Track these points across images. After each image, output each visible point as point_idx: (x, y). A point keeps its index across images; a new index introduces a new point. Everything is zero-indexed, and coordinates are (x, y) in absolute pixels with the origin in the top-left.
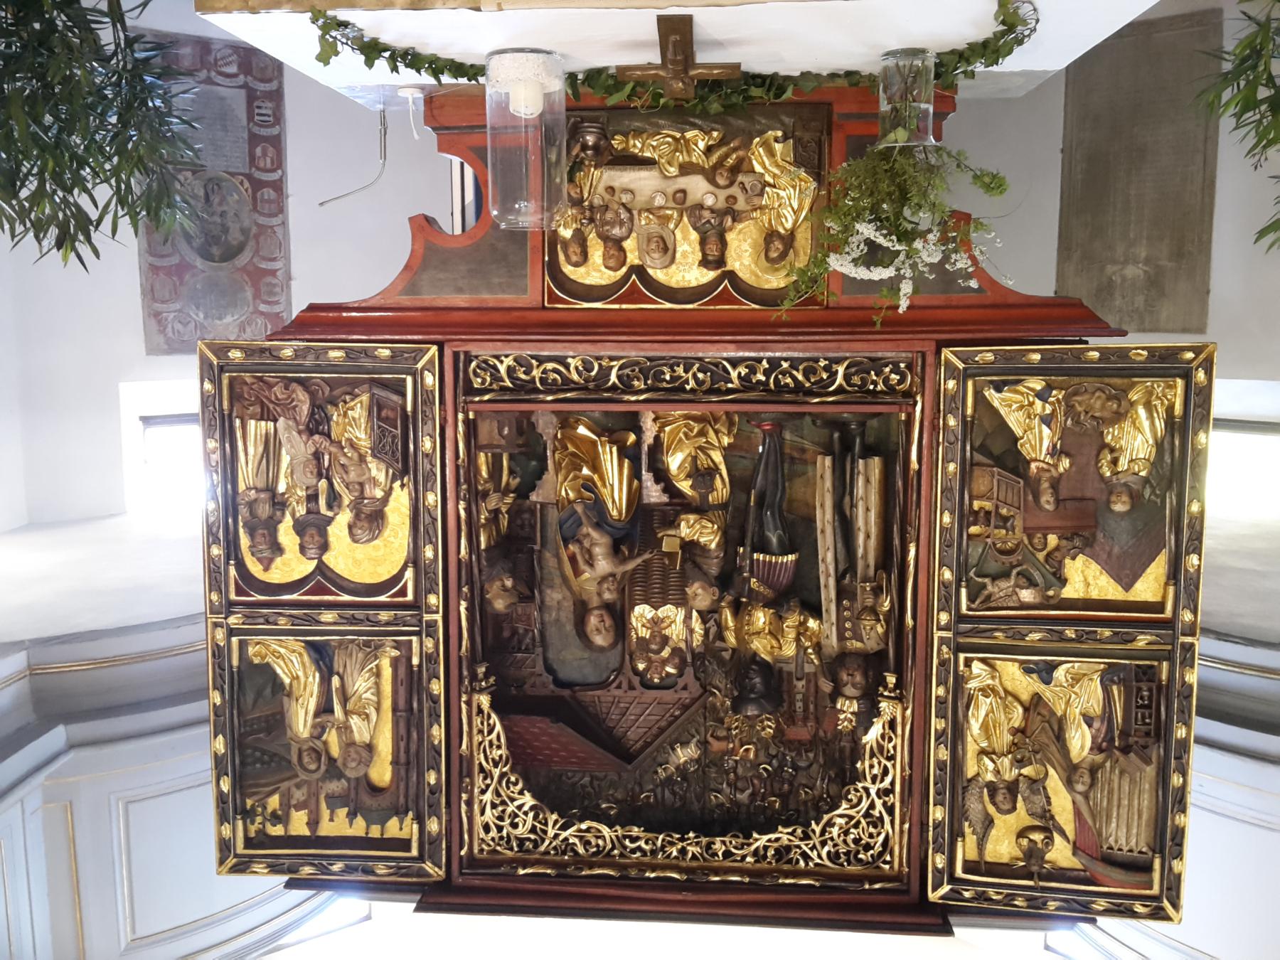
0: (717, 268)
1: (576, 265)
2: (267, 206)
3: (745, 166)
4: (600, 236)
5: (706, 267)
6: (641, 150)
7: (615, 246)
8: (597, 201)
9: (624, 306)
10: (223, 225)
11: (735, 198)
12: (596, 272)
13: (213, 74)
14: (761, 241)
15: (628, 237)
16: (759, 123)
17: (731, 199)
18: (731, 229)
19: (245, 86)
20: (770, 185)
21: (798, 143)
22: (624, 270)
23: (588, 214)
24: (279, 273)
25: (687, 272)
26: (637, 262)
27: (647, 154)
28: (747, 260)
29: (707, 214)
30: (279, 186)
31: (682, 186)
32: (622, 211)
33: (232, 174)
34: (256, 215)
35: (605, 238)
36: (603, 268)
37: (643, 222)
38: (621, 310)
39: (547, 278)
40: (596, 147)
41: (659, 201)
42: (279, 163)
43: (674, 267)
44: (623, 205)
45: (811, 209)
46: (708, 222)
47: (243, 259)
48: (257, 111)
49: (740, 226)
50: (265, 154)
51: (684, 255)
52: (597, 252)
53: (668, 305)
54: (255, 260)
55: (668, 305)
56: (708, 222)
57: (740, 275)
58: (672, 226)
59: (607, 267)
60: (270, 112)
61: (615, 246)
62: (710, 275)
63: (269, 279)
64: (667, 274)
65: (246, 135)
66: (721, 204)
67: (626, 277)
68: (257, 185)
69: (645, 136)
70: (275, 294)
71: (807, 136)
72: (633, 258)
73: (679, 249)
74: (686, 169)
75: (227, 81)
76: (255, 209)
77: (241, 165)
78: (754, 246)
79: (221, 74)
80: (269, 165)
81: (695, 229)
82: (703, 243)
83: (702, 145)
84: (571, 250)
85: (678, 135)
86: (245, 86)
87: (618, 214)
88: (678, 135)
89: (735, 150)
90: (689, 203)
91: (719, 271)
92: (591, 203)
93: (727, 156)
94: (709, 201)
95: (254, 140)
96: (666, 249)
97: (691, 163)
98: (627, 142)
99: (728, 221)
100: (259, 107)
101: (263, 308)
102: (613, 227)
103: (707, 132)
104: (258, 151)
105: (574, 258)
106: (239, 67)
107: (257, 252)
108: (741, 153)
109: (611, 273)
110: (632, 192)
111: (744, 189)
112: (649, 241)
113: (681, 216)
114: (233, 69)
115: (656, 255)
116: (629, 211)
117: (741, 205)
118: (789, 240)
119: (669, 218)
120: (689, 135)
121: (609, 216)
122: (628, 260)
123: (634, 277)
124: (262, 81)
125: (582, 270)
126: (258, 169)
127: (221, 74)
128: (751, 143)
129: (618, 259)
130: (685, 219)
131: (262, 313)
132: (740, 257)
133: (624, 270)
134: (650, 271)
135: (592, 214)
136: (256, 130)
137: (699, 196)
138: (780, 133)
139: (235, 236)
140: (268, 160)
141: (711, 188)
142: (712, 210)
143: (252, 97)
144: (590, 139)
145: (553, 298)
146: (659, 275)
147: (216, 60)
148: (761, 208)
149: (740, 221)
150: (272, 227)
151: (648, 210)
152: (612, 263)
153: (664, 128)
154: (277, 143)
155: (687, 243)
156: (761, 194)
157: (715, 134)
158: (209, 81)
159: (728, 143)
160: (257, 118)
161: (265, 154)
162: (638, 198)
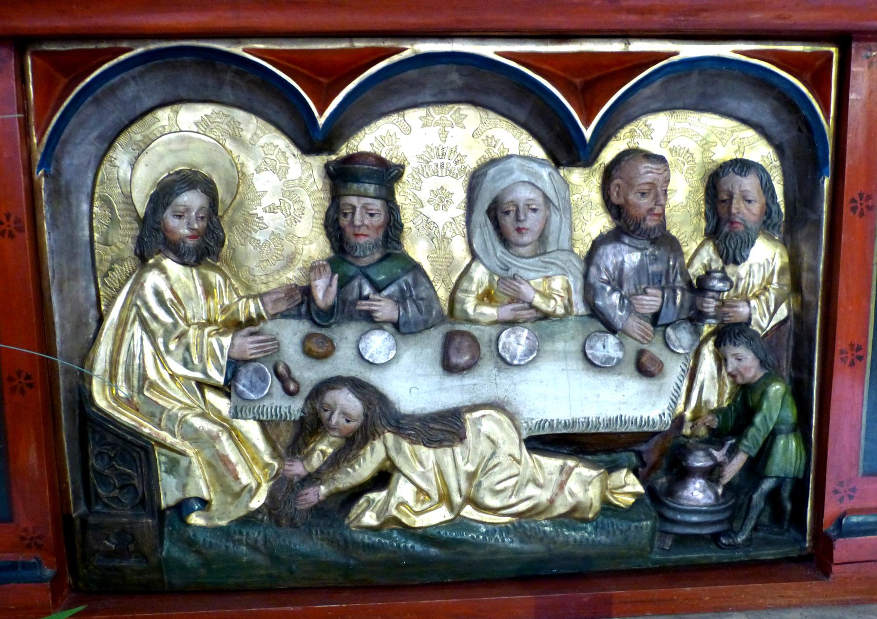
0: (350, 159)
1: (742, 166)
3: (285, 436)
4: (672, 245)
5: (381, 162)
6: (566, 472)
7: (631, 220)
8: (682, 338)
9: (616, 46)
11: (308, 353)
12: (687, 143)
14: (232, 237)
15: (597, 244)
16: (254, 548)
17: (317, 350)
18: (314, 269)
20: (216, 388)
21: (147, 498)
22: (608, 155)
23: (710, 305)
25: (438, 150)
26: (576, 176)
27: (552, 464)
28: (265, 185)
29: (385, 309)
31: (453, 381)
32: (618, 316)
35: (663, 241)
36: (669, 158)
37: (558, 283)
38: (626, 35)
39: (829, 127)
40: (682, 474)
41: (516, 342)
43: (472, 163)
44: (611, 329)
45: (101, 320)
46: (378, 288)
49: (292, 276)
51: (442, 198)
52: (682, 205)
53: (488, 50)
55: (488, 50)
56: (378, 288)
57: (282, 142)
58: (480, 273)
59: (661, 159)
61: (631, 220)
62: (368, 140)
64: (490, 141)
66: (345, 335)
67: (604, 135)
69: (560, 508)
71: (124, 515)
72: (584, 184)
73: (457, 210)
74: (443, 428)
78: (249, 223)
81: (416, 268)
82: (393, 228)
83: (404, 490)
84: (756, 208)
85: (469, 512)
87: (628, 303)
88: (469, 512)
89: (313, 478)
90: (436, 336)
91: (343, 152)
92: (697, 332)
93: (336, 462)
94: (378, 344)
96: (495, 212)
97: (430, 443)
98: (604, 488)
99: (324, 291)
102: (640, 269)
103: (391, 523)
105: (749, 184)
108: (298, 469)
109: (644, 145)
110: (590, 363)
111: (285, 378)
112: (542, 238)
113: (452, 300)
115: (524, 194)
116: (595, 313)
117: (290, 334)
118: (153, 240)
119: (487, 297)
120: (442, 515)
121: (651, 301)
122: (596, 180)
123: (588, 133)
125: (723, 154)
128: (271, 495)
129: (630, 185)
130: (443, 294)
132: (289, 192)
133: (608, 155)
134: (539, 152)
135: (696, 305)
137: (408, 357)
138: (196, 519)
141: (374, 378)
142: (370, 319)
144: (697, 493)
145: (814, 71)
146: (513, 140)
148: (234, 325)
149: (290, 290)
151: (546, 316)
152: (646, 173)
153: (504, 529)
155: (434, 226)
156: (235, 366)
157: (370, 519)
159: (331, 496)
162: (574, 346)
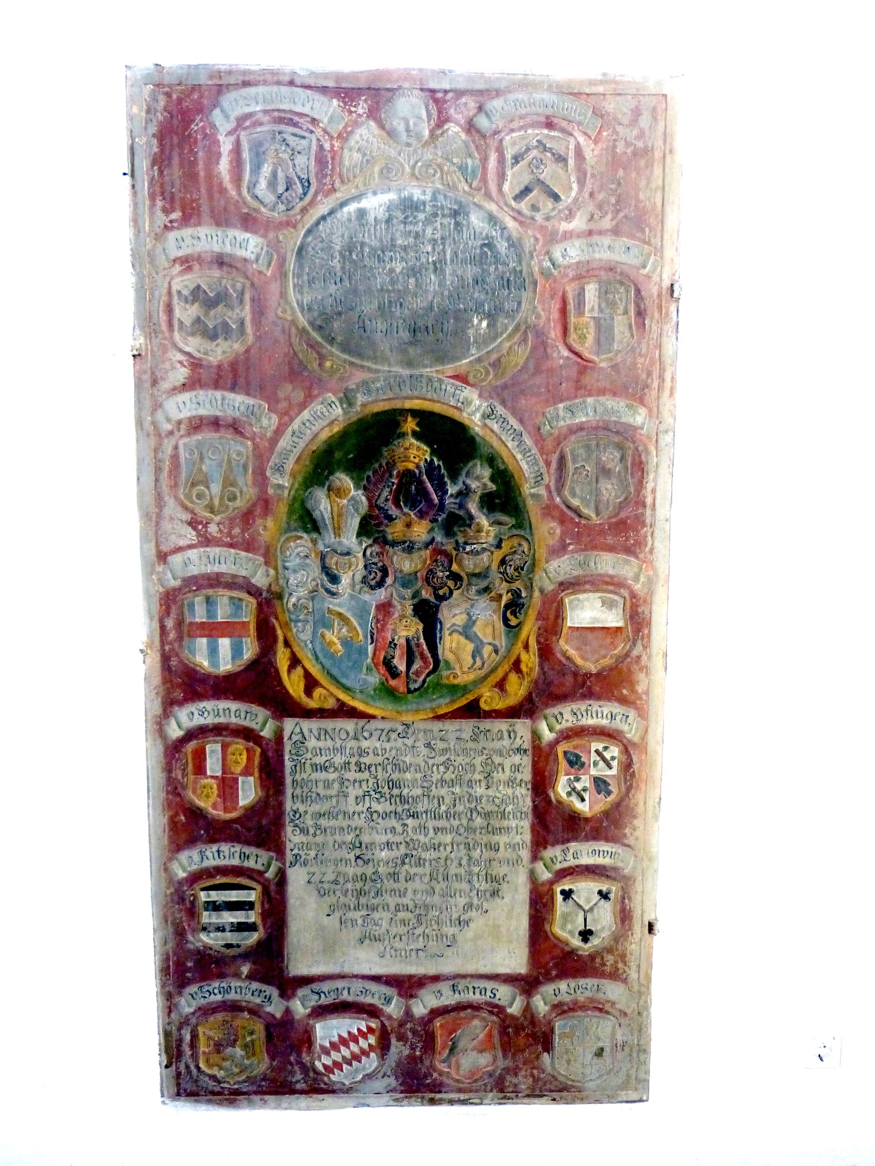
2: (222, 614)
10: (383, 541)
13: (394, 1009)
19: (289, 986)
24: (181, 374)
30: (182, 683)
33: (344, 711)
34: (260, 580)
42: (179, 756)
47: (322, 418)
48: (252, 917)
50: (227, 786)
54: (269, 422)
60: (207, 917)
63: (219, 352)
65: (292, 838)
68: (256, 683)
70: (197, 294)
75: (352, 992)
76: (268, 604)
77: (309, 741)
79: (372, 1012)
80: (213, 751)
86: (289, 986)
95: (263, 827)
100: (241, 927)
101: (248, 245)
104: (248, 792)
106: (308, 1039)
107: (261, 457)
114: (326, 1031)
124: (234, 1007)
126: (247, 734)
127: (372, 1012)
131: (248, 222)
136: (257, 858)
139: (344, 501)
140: (213, 766)
143: (267, 957)
147: (384, 1047)
150: (207, 541)
154: (186, 825)
158: (407, 986)
160: (252, 896)
161: (227, 786)
